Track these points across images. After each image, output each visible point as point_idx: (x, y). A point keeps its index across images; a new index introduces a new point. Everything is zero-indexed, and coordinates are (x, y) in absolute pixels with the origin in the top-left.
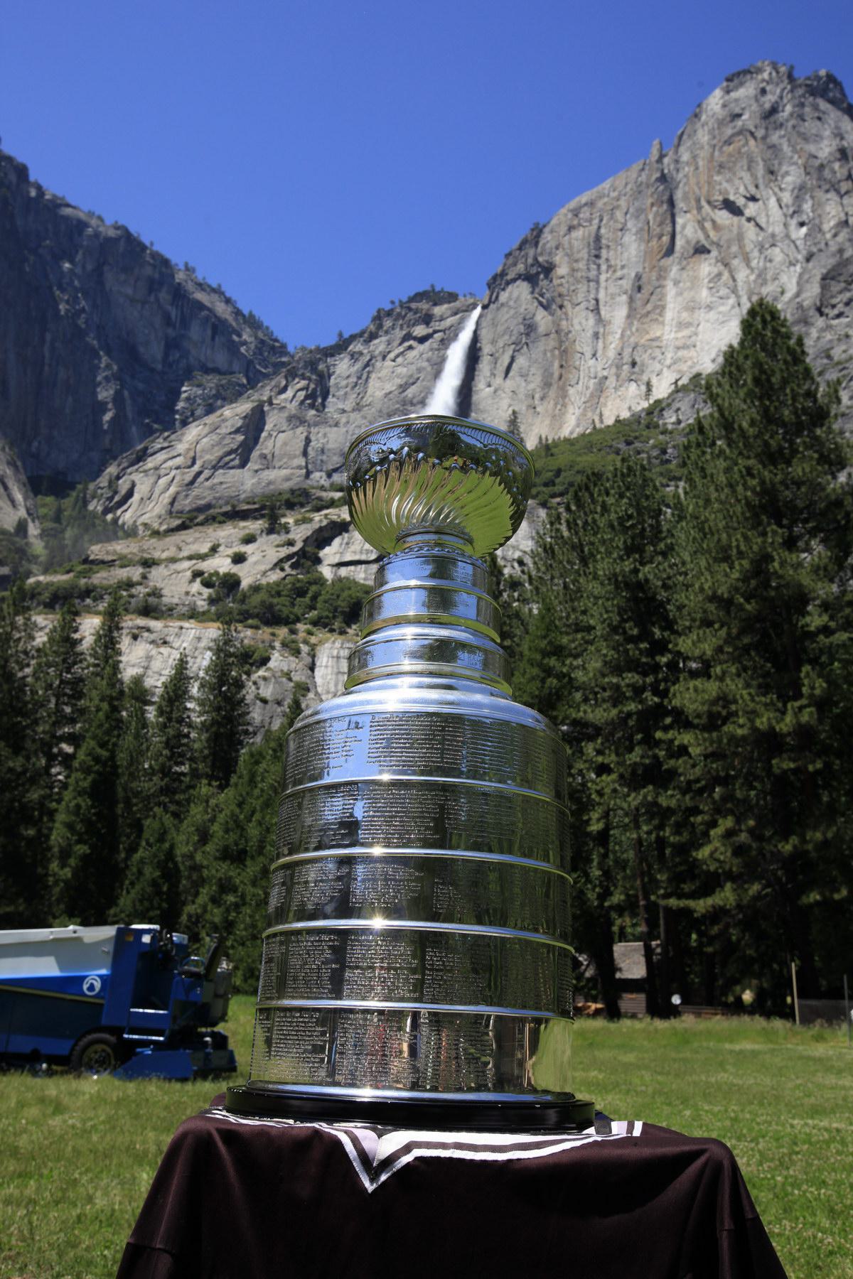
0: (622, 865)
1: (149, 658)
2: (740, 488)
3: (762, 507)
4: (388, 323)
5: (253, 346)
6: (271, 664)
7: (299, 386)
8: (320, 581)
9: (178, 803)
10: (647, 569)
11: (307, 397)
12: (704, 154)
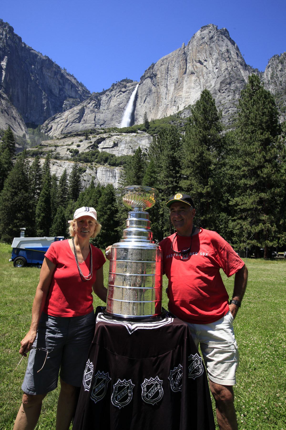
0: (166, 220)
1: (57, 169)
2: (198, 136)
3: (202, 140)
4: (115, 87)
5: (81, 91)
6: (86, 172)
7: (93, 102)
8: (98, 152)
9: (65, 204)
10: (176, 153)
11: (95, 105)
12: (195, 48)
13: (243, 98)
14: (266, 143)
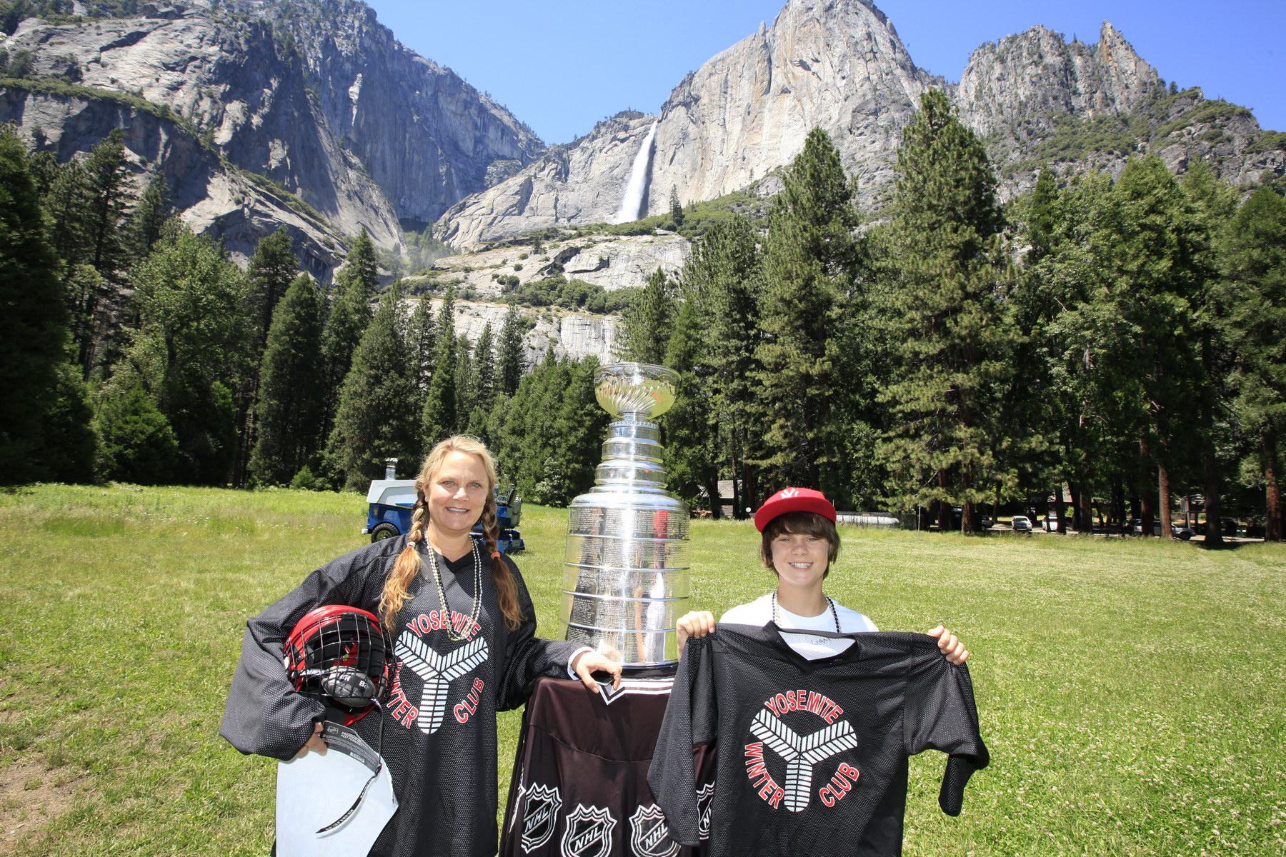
0: (724, 440)
1: (470, 324)
2: (799, 238)
3: (810, 248)
4: (603, 130)
8: (563, 282)
9: (488, 404)
10: (746, 281)
11: (556, 174)
12: (790, 31)
13: (907, 146)
14: (967, 252)
